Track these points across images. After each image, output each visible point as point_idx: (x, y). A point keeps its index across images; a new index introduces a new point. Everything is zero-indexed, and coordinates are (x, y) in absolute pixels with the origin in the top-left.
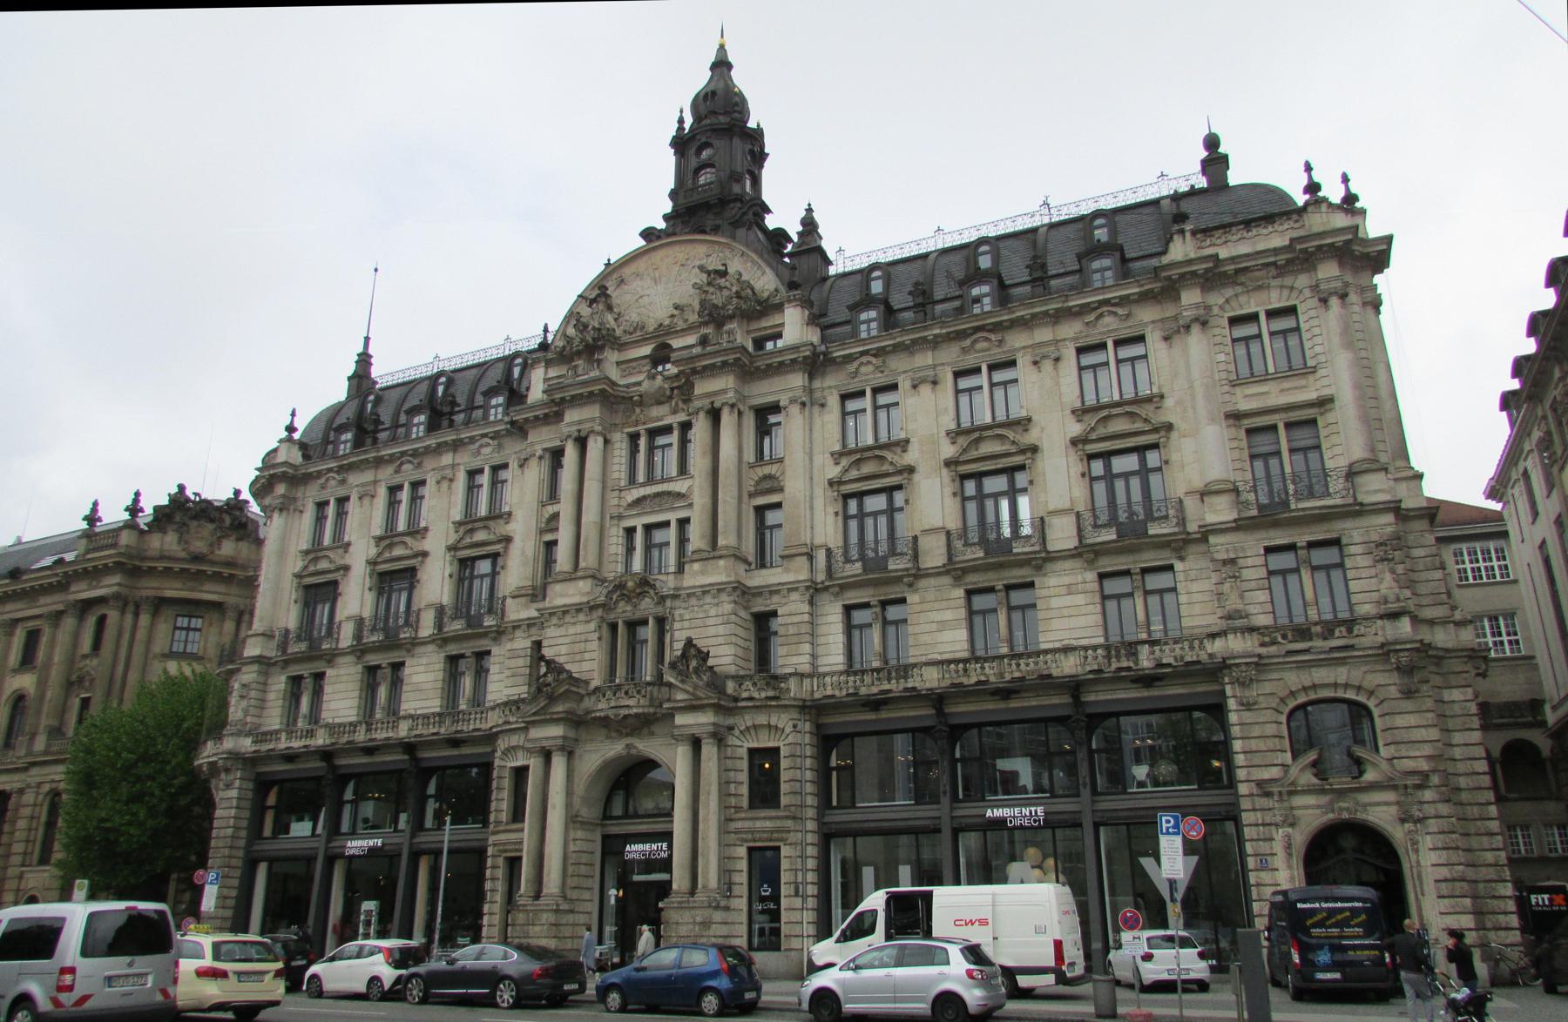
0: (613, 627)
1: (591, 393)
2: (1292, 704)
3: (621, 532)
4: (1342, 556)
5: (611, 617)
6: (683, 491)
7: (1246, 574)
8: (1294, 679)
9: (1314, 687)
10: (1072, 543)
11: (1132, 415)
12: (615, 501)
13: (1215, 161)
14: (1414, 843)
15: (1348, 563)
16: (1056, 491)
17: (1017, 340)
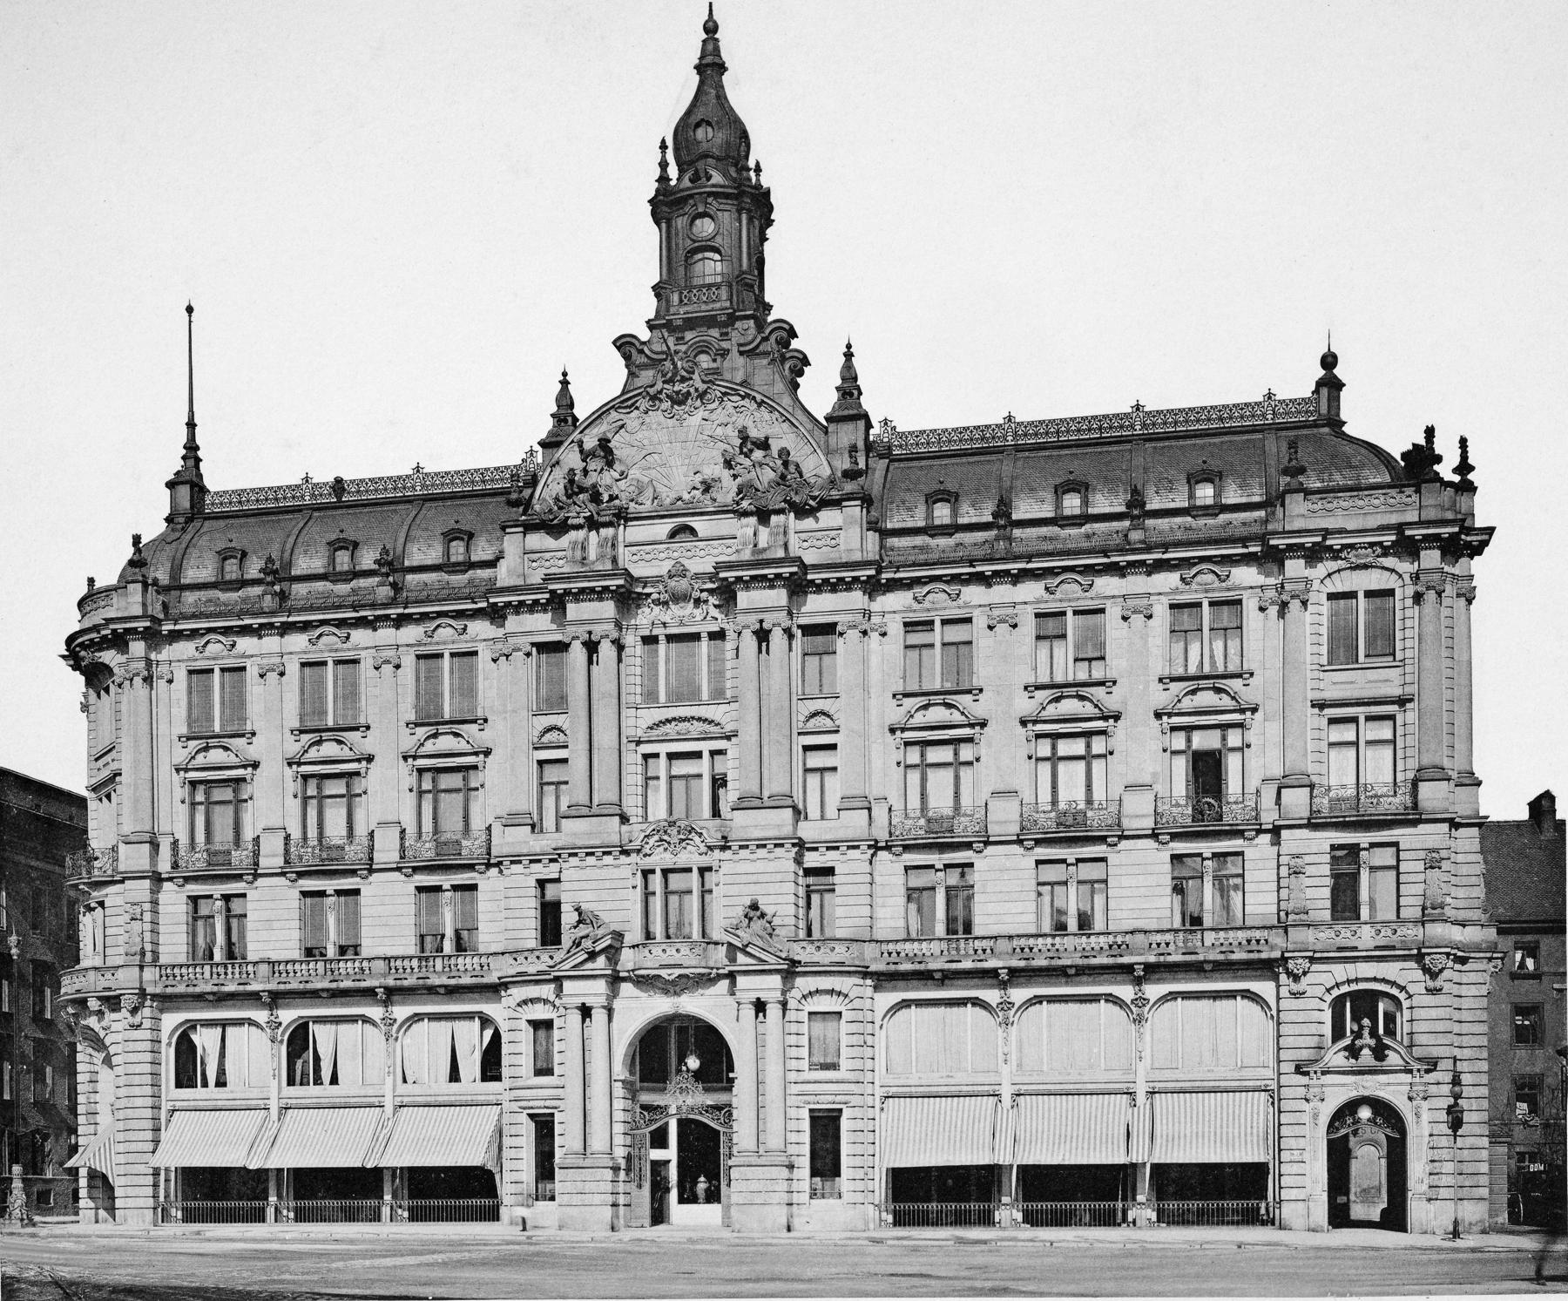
0: (646, 873)
1: (606, 588)
2: (1336, 992)
3: (640, 759)
4: (1398, 860)
5: (647, 863)
6: (717, 719)
7: (1310, 870)
8: (1340, 972)
9: (1357, 980)
10: (1149, 823)
11: (1218, 691)
12: (632, 722)
13: (1331, 385)
14: (1418, 1115)
15: (1403, 867)
16: (1142, 769)
17: (1107, 585)
